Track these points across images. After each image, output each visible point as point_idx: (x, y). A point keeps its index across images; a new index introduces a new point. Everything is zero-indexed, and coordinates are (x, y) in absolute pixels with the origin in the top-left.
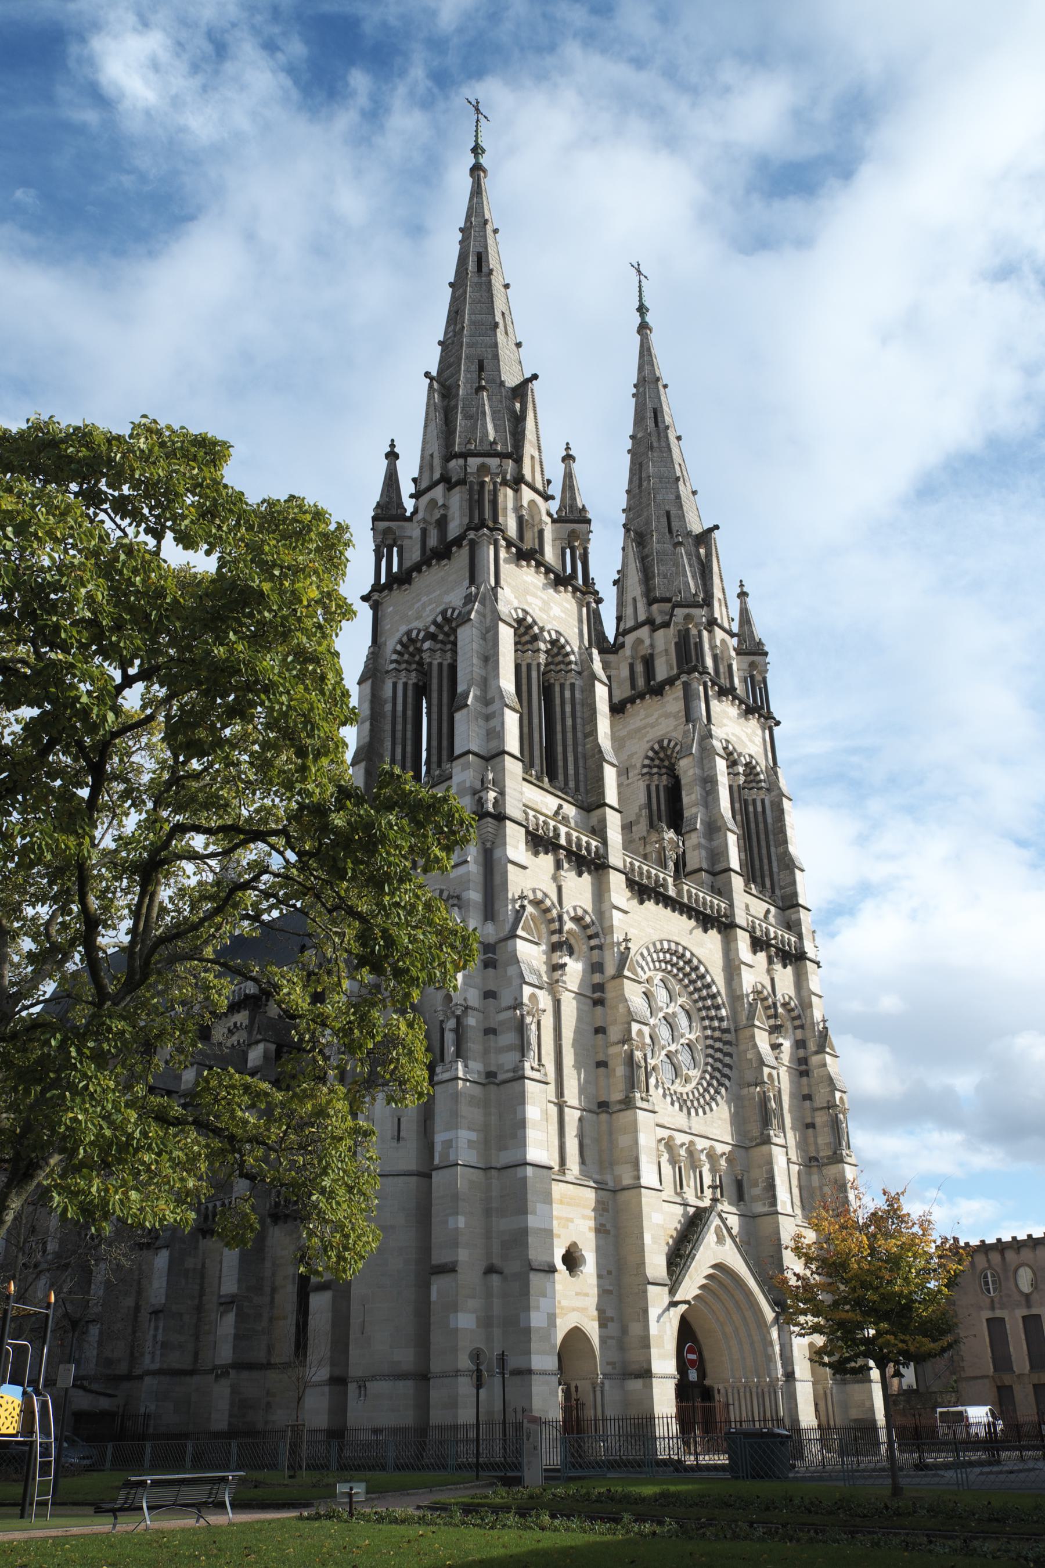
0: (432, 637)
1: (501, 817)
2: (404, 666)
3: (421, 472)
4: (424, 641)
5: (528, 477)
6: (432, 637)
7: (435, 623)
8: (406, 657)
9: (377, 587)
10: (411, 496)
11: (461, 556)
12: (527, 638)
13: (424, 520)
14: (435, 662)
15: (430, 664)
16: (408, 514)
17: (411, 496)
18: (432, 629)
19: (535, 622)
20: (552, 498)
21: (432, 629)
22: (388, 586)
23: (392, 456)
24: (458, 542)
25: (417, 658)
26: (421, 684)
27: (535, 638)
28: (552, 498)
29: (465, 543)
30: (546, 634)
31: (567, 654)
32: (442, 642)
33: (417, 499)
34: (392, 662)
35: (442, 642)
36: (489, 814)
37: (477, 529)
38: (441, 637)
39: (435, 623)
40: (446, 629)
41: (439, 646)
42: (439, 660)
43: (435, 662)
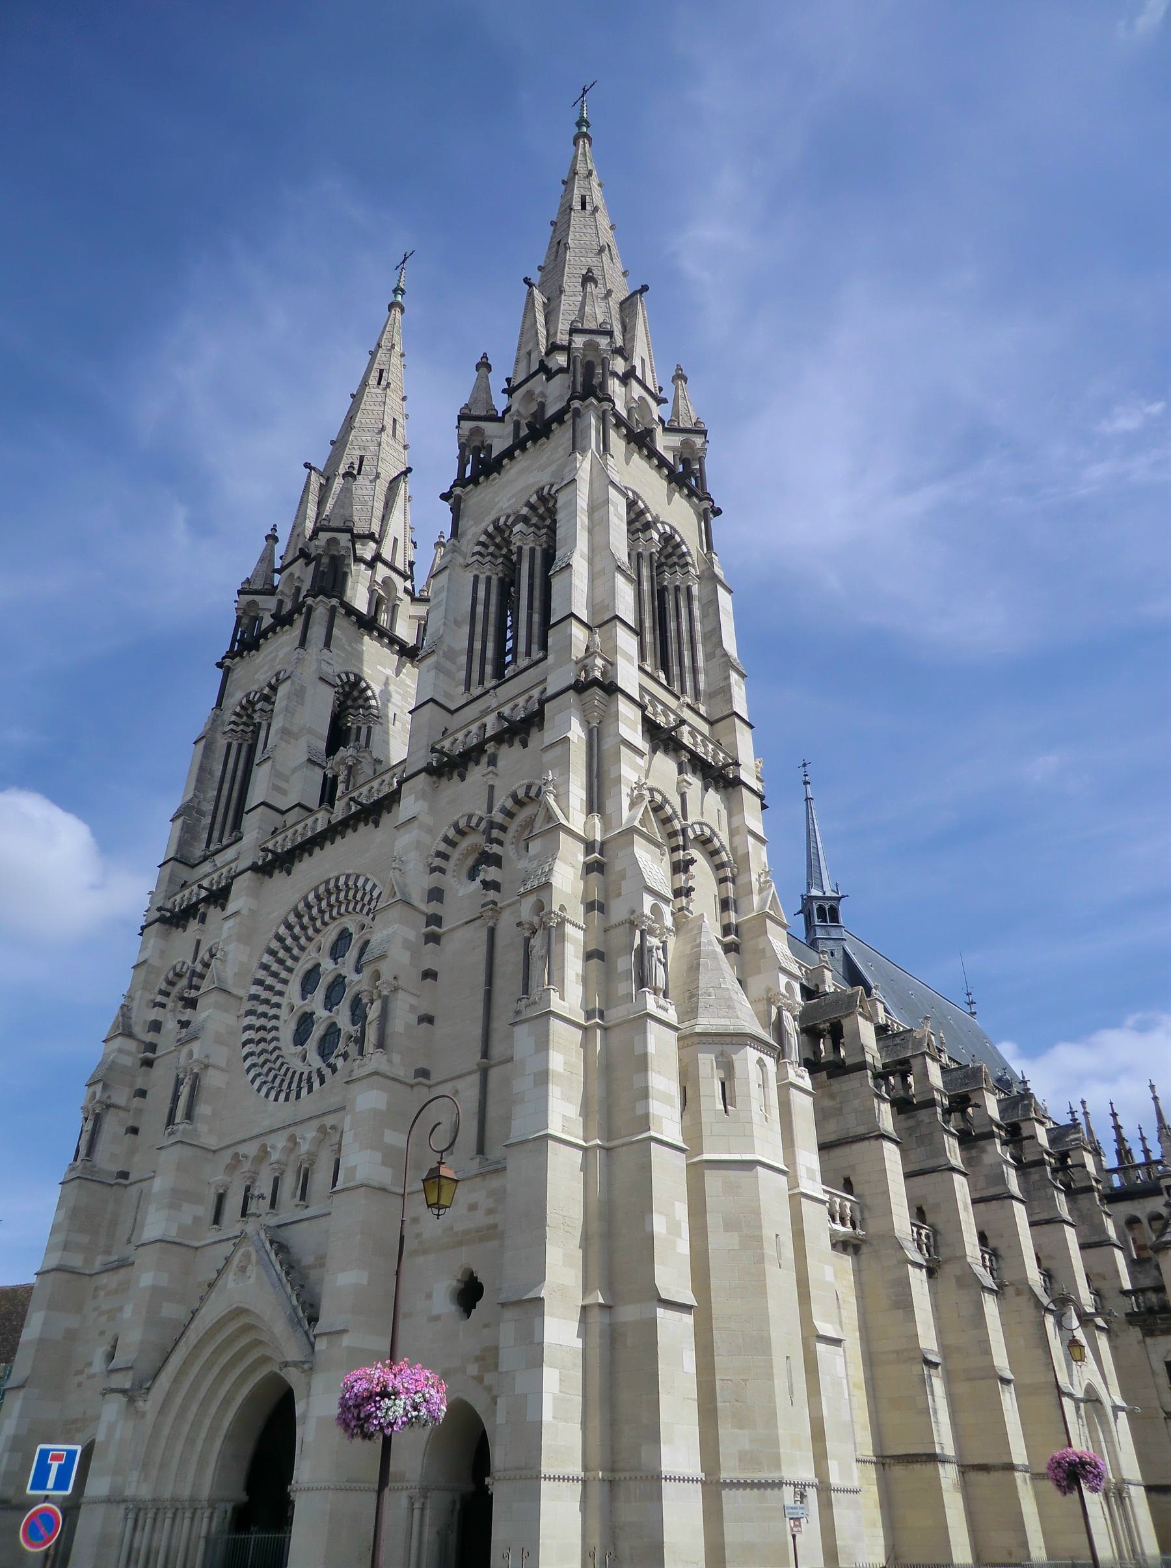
0: (525, 520)
1: (611, 689)
2: (489, 558)
3: (515, 372)
4: (514, 524)
5: (639, 373)
6: (525, 520)
8: (492, 549)
9: (461, 482)
10: (504, 391)
11: (561, 436)
12: (638, 525)
13: (518, 413)
15: (520, 549)
16: (500, 415)
17: (504, 391)
18: (525, 511)
19: (647, 509)
20: (665, 401)
21: (525, 511)
22: (474, 480)
23: (484, 365)
24: (559, 417)
25: (504, 551)
26: (507, 580)
27: (647, 526)
28: (665, 401)
30: (659, 525)
31: (683, 555)
32: (535, 525)
33: (510, 396)
35: (535, 525)
36: (595, 682)
37: (583, 398)
38: (534, 520)
40: (541, 510)
41: (532, 529)
42: (532, 545)
43: (526, 548)
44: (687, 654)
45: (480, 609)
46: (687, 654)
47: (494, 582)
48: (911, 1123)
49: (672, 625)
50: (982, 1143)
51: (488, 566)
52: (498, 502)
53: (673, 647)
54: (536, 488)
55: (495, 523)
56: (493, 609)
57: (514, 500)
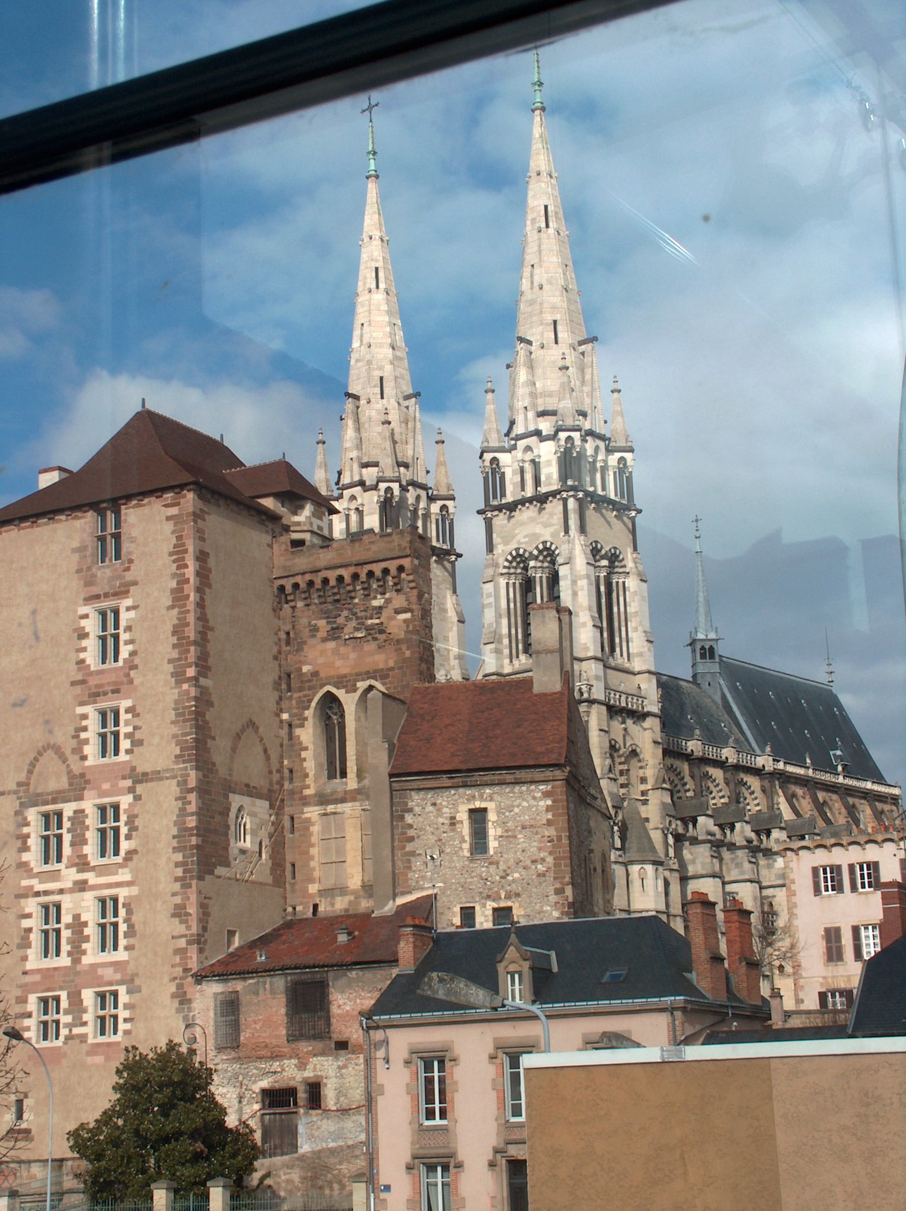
7: (537, 548)
14: (538, 576)
21: (535, 552)
29: (558, 497)
34: (505, 567)
39: (537, 548)
41: (539, 564)
43: (538, 576)
44: (623, 629)
45: (512, 605)
46: (623, 629)
47: (517, 585)
48: (733, 856)
49: (615, 609)
50: (775, 857)
51: (513, 577)
52: (517, 535)
53: (616, 624)
54: (542, 539)
55: (517, 549)
56: (518, 605)
57: (527, 540)
